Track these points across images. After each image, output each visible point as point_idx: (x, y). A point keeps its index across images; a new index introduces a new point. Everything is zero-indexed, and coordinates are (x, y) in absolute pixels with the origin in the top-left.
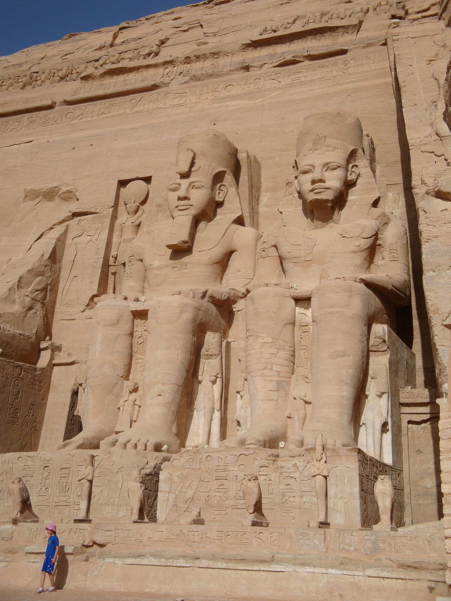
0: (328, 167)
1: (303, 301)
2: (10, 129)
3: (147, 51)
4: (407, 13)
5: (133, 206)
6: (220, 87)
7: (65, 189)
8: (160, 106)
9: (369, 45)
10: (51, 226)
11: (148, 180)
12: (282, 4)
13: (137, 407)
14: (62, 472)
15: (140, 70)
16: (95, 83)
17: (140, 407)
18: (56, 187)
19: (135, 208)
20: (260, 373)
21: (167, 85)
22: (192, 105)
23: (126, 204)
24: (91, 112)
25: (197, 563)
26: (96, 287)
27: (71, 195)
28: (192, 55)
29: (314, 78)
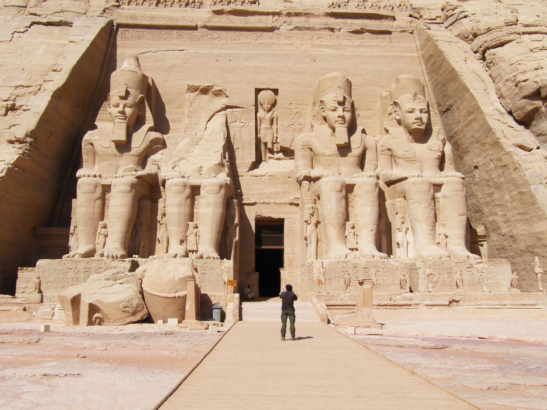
0: (421, 111)
1: (437, 187)
2: (163, 38)
4: (421, 17)
5: (267, 106)
6: (315, 37)
7: (216, 88)
8: (276, 42)
9: (403, 31)
11: (276, 91)
16: (222, 16)
20: (425, 221)
21: (278, 29)
23: (261, 105)
25: (505, 307)
27: (221, 93)
28: (292, 11)
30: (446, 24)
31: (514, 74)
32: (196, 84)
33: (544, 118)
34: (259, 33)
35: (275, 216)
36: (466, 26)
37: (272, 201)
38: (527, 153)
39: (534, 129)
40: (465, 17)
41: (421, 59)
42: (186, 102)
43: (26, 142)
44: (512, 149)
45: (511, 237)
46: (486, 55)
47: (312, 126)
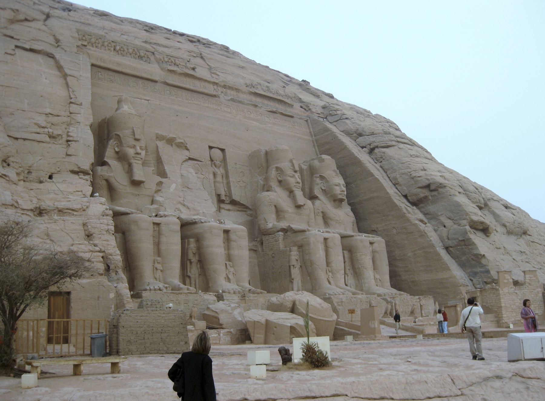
1: (371, 243)
3: (192, 67)
4: (310, 109)
7: (179, 140)
8: (219, 108)
9: (301, 119)
11: (223, 150)
30: (330, 119)
31: (409, 170)
32: (164, 134)
33: (430, 203)
36: (350, 125)
38: (424, 226)
39: (423, 210)
40: (346, 118)
41: (315, 142)
42: (160, 150)
43: (89, 174)
44: (417, 222)
45: (413, 282)
46: (376, 151)
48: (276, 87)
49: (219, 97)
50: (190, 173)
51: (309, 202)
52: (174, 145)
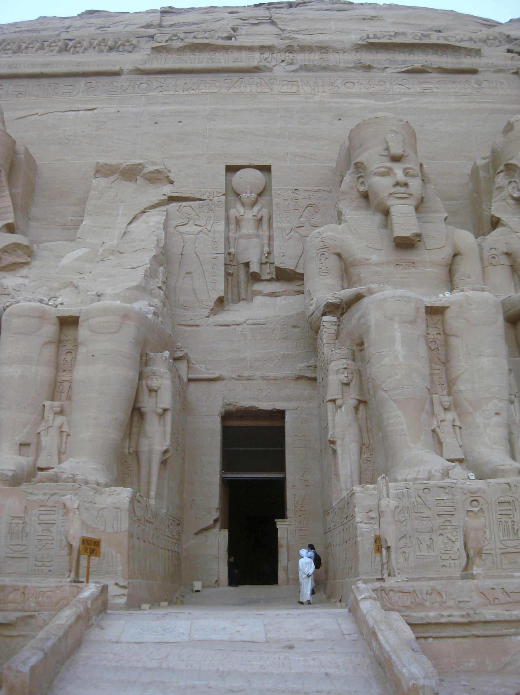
5: (248, 196)
6: (339, 82)
8: (266, 90)
10: (142, 209)
11: (266, 169)
12: (364, 19)
13: (457, 429)
14: (502, 508)
15: (230, 51)
17: (460, 428)
18: (140, 164)
19: (254, 200)
21: (270, 70)
22: (307, 96)
24: (174, 86)
26: (222, 287)
29: (448, 91)
34: (235, 77)
35: (266, 405)
37: (258, 374)
42: (92, 192)
47: (340, 214)
48: (457, 36)
49: (270, 70)
50: (147, 223)
51: (465, 238)
52: (140, 180)
